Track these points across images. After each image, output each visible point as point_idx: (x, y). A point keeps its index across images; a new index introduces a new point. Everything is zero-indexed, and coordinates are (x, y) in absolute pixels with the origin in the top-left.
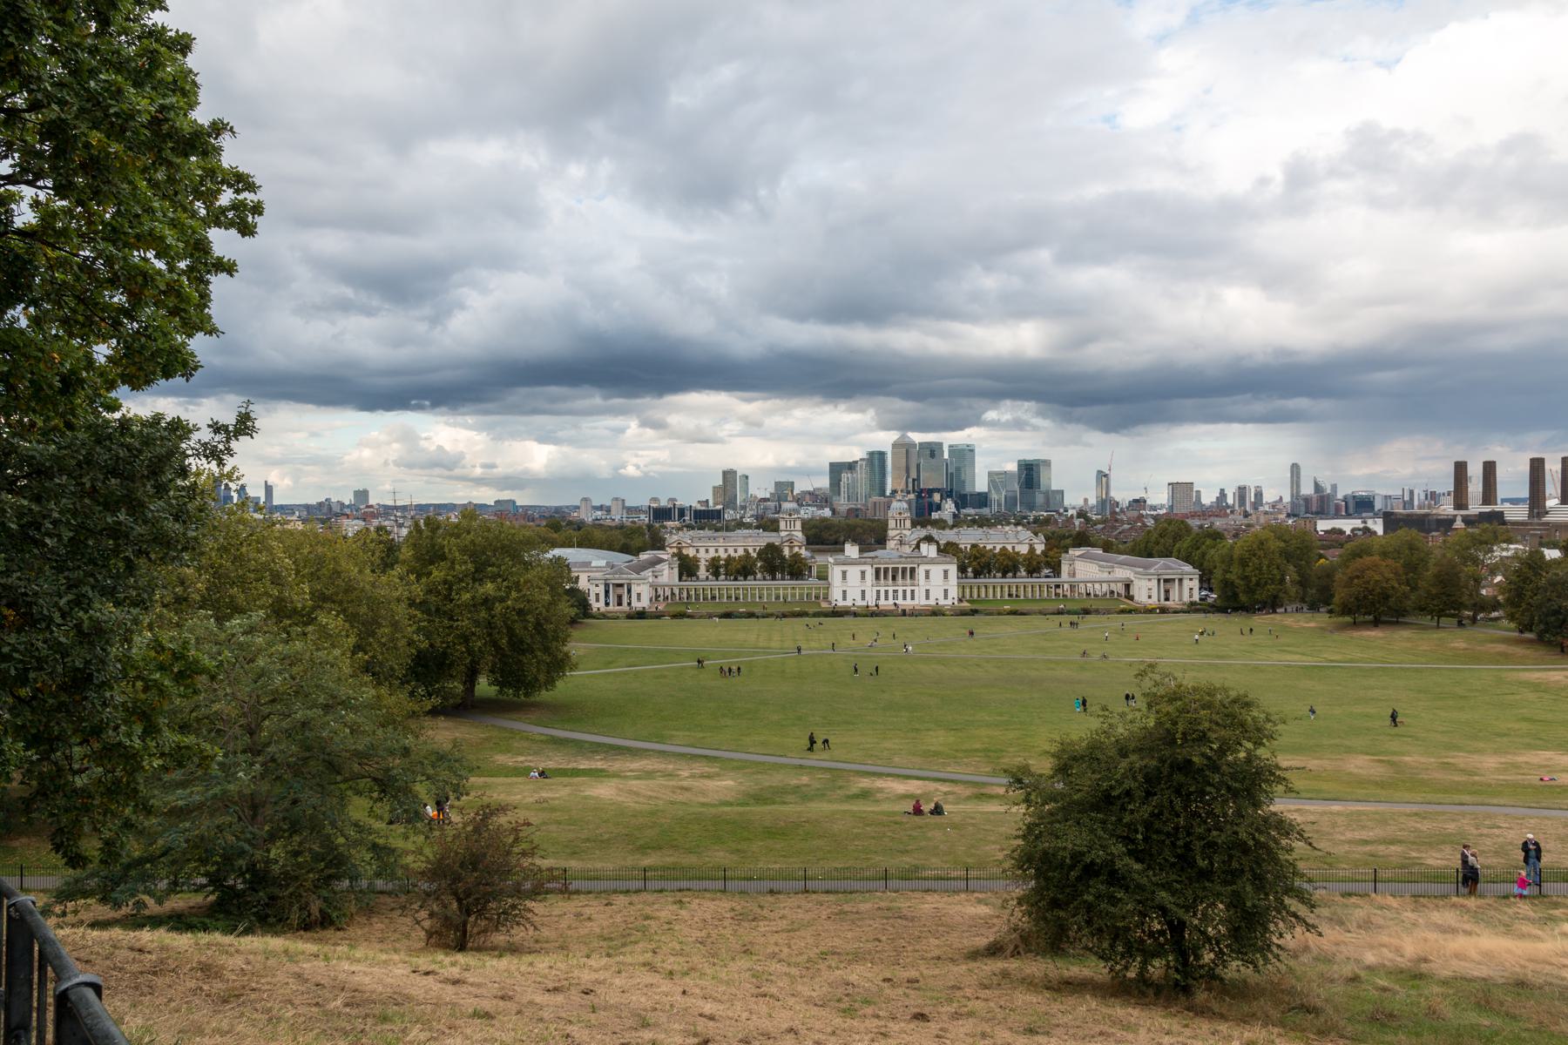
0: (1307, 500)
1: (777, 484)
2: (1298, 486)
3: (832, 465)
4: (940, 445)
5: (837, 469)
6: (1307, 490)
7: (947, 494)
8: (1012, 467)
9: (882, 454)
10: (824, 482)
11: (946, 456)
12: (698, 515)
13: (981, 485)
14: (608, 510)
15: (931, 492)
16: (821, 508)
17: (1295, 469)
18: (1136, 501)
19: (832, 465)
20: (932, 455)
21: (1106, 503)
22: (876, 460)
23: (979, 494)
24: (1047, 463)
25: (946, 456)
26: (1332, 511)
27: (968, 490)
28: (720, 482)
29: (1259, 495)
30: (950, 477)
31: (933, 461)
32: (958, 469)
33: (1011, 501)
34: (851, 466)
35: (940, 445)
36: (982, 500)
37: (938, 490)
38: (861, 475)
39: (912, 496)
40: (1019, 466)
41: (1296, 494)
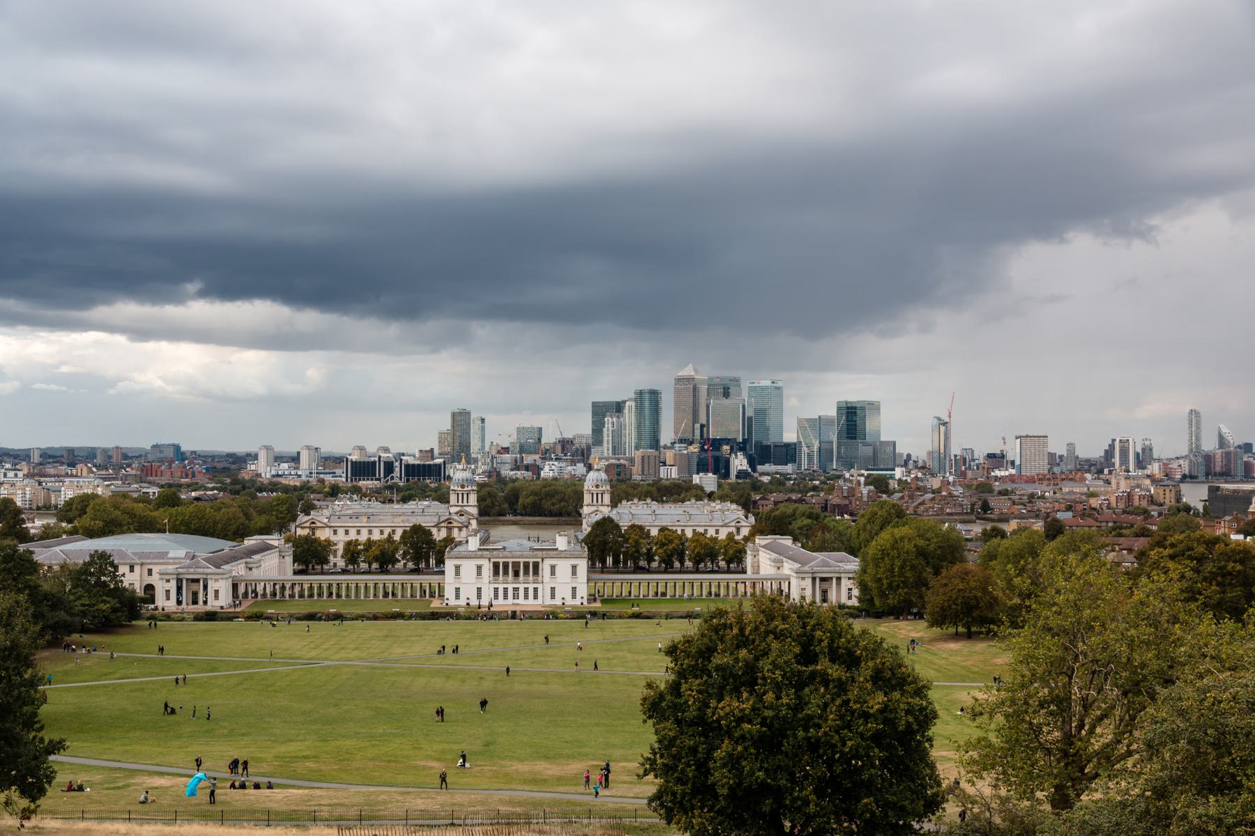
0: (1208, 458)
1: (520, 431)
2: (1198, 438)
3: (595, 405)
4: (736, 381)
5: (601, 411)
6: (1209, 444)
7: (742, 447)
8: (833, 412)
9: (654, 394)
10: (581, 427)
11: (745, 395)
12: (411, 470)
13: (790, 436)
14: (295, 459)
15: (717, 444)
16: (573, 463)
17: (1194, 416)
18: (991, 456)
19: (595, 405)
20: (726, 394)
21: (941, 459)
22: (650, 401)
23: (787, 445)
24: (875, 407)
25: (745, 395)
26: (1240, 471)
27: (772, 439)
28: (446, 425)
29: (1147, 450)
30: (748, 423)
31: (725, 402)
32: (761, 413)
33: (825, 454)
34: (619, 407)
35: (736, 381)
36: (788, 453)
37: (727, 441)
38: (629, 416)
39: (694, 449)
40: (839, 409)
41: (1195, 450)
